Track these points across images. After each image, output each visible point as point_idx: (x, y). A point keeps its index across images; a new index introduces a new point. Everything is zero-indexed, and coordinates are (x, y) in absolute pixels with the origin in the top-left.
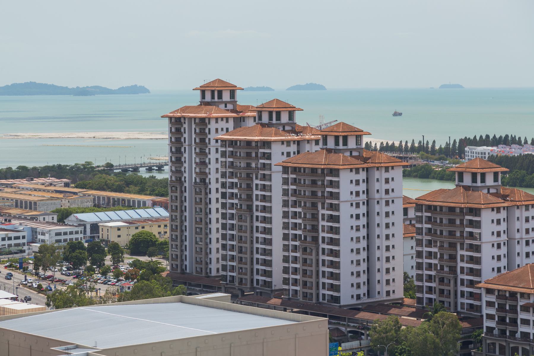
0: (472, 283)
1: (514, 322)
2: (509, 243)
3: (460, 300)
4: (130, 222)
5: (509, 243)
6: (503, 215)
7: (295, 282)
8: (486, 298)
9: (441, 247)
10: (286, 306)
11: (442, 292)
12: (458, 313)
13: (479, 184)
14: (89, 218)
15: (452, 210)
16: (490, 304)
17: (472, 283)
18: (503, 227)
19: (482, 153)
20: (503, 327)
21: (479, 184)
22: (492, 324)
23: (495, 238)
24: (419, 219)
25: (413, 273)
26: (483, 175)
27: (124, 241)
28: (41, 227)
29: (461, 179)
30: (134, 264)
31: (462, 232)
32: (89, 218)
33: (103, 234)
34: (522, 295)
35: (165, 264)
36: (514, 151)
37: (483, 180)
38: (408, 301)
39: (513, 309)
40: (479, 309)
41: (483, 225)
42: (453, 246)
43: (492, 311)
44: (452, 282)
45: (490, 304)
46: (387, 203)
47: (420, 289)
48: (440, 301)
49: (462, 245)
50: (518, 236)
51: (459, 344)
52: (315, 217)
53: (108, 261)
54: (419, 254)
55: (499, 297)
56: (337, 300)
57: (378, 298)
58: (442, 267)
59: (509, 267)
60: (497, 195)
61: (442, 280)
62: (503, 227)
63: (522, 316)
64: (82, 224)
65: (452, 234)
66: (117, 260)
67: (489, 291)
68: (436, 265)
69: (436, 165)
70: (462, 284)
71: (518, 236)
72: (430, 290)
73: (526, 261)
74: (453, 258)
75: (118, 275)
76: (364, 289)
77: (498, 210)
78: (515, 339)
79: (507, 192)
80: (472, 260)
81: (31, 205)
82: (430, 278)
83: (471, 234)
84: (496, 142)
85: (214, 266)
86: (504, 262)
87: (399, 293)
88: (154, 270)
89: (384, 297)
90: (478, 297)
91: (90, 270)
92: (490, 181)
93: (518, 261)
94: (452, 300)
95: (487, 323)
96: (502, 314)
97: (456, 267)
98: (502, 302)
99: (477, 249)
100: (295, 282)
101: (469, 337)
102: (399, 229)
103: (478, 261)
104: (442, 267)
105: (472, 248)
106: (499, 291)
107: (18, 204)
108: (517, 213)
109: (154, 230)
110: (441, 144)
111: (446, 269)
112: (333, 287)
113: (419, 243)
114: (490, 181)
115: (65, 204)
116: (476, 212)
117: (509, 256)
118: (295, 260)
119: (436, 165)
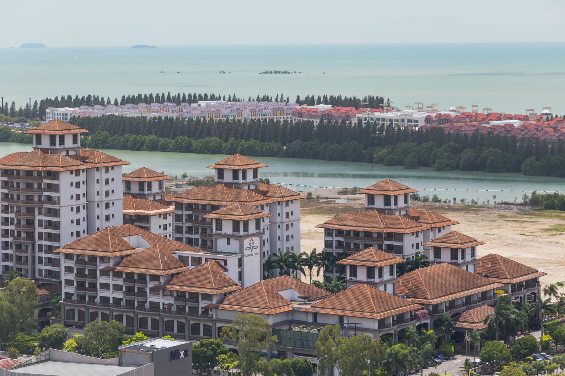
0: (50, 249)
1: (93, 286)
3: (38, 267)
5: (88, 206)
6: (82, 177)
8: (64, 263)
9: (19, 212)
11: (19, 259)
12: (36, 280)
13: (58, 146)
15: (29, 173)
16: (69, 270)
17: (50, 249)
18: (83, 189)
19: (63, 115)
20: (82, 292)
21: (58, 146)
22: (71, 290)
23: (74, 202)
26: (62, 138)
29: (39, 142)
31: (40, 197)
34: (102, 259)
36: (97, 112)
37: (62, 142)
39: (93, 274)
40: (57, 275)
41: (62, 188)
42: (30, 211)
44: (30, 249)
45: (69, 270)
46: (107, 206)
48: (18, 269)
49: (40, 209)
50: (97, 199)
51: (36, 311)
55: (77, 262)
58: (19, 233)
59: (88, 231)
60: (76, 157)
61: (19, 247)
62: (83, 189)
63: (101, 280)
65: (29, 198)
67: (68, 256)
68: (13, 231)
69: (16, 128)
70: (40, 249)
71: (97, 199)
73: (106, 224)
74: (30, 223)
77: (78, 173)
78: (94, 304)
79: (87, 154)
80: (50, 224)
83: (49, 198)
84: (78, 102)
86: (83, 226)
90: (56, 263)
92: (68, 142)
93: (98, 224)
94: (29, 267)
95: (66, 289)
96: (81, 279)
97: (33, 233)
98: (81, 266)
99: (56, 213)
101: (47, 304)
103: (56, 225)
104: (19, 233)
106: (78, 256)
108: (97, 175)
110: (20, 105)
111: (23, 235)
114: (68, 142)
116: (54, 175)
117: (88, 219)
119: (16, 128)
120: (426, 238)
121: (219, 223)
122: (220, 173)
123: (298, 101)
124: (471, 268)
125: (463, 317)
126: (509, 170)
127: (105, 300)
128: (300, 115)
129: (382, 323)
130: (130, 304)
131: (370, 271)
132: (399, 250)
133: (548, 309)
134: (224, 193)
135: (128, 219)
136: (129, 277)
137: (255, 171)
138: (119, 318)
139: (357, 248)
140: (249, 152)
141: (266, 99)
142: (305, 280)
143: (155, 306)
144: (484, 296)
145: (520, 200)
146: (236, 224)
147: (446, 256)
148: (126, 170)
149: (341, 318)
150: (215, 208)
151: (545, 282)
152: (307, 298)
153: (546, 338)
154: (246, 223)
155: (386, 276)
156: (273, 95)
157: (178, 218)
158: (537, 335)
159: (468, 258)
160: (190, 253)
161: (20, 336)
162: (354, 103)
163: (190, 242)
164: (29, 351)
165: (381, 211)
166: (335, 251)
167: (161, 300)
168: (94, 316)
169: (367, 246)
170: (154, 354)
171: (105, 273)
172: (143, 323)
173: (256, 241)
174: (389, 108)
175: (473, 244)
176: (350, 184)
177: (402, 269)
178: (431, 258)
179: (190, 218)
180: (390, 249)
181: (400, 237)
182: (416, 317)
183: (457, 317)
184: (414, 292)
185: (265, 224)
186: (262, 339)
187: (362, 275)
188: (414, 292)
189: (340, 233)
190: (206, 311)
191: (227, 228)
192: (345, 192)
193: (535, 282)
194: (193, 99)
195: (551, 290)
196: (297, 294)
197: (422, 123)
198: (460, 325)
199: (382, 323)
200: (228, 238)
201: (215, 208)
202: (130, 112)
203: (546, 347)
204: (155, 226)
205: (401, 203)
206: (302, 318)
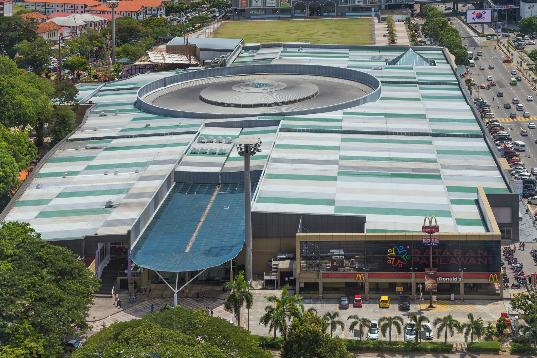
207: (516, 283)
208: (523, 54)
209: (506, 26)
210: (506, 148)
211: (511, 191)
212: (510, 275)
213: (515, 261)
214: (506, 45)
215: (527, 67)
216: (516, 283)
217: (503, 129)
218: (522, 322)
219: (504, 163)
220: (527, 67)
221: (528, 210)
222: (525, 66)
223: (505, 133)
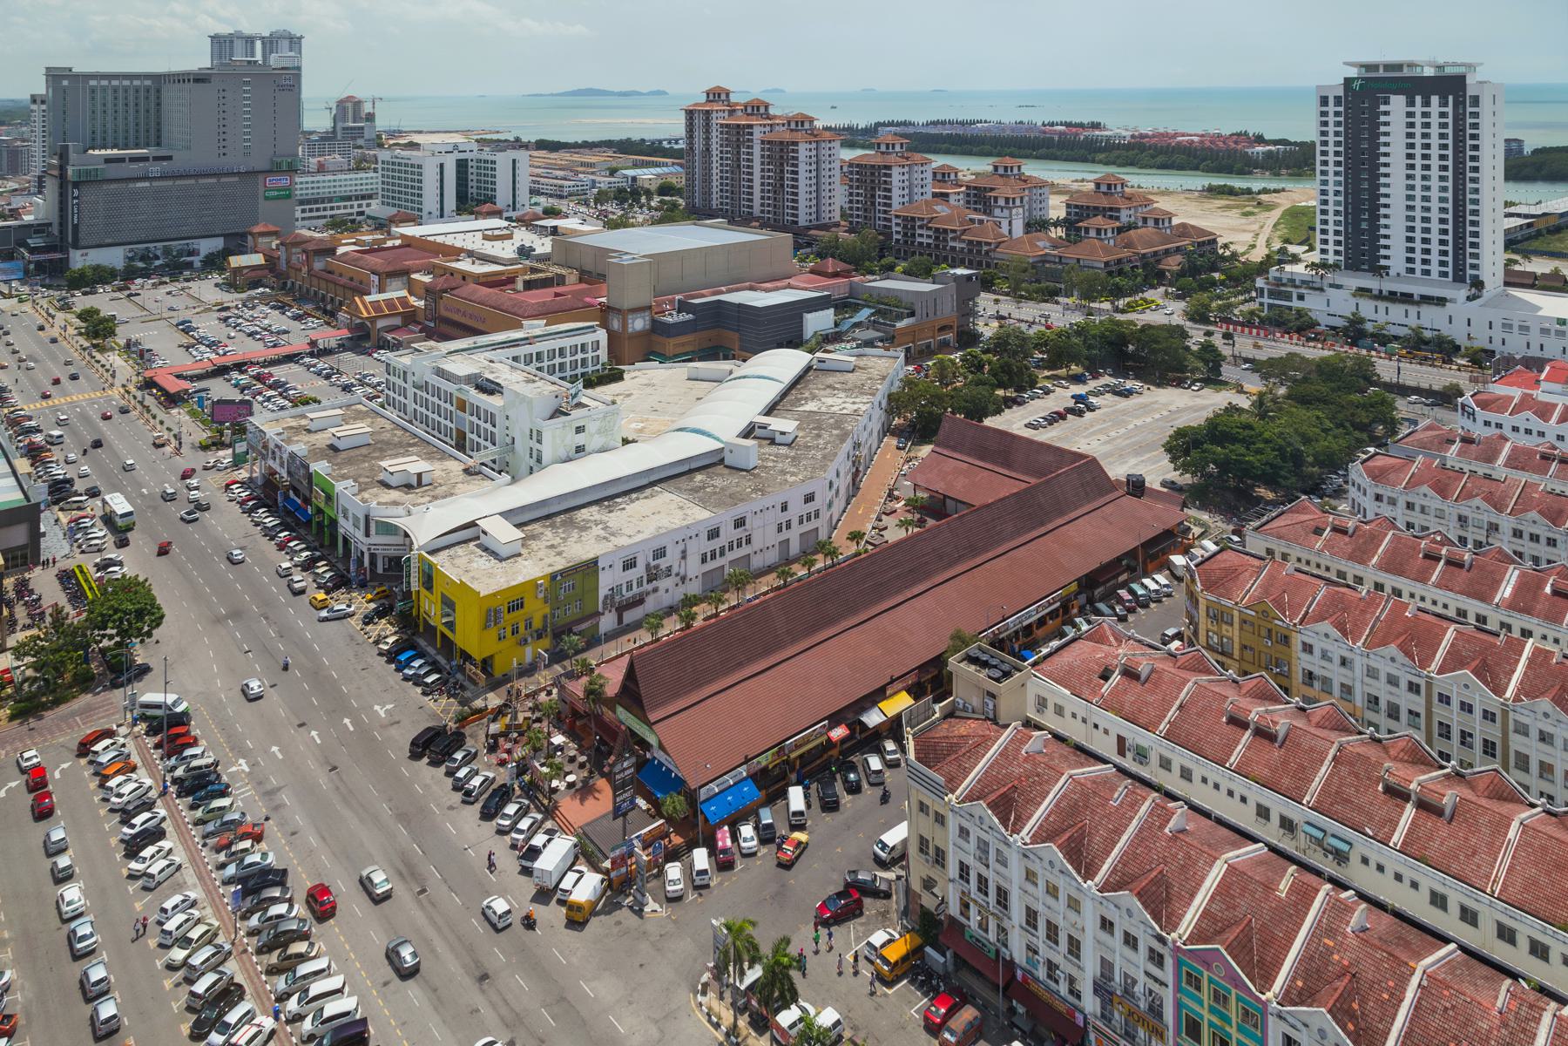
0: (885, 212)
1: (913, 235)
2: (910, 187)
4: (658, 175)
5: (910, 187)
6: (906, 169)
7: (769, 212)
8: (894, 221)
10: (761, 227)
14: (631, 173)
16: (897, 224)
17: (885, 212)
18: (906, 177)
22: (899, 237)
24: (851, 173)
25: (847, 206)
27: (653, 188)
28: (598, 179)
30: (661, 202)
32: (631, 173)
33: (639, 183)
35: (681, 201)
38: (843, 223)
39: (913, 228)
40: (890, 227)
42: (873, 189)
43: (899, 229)
45: (897, 224)
47: (851, 216)
52: (782, 171)
53: (643, 200)
54: (851, 194)
56: (796, 223)
57: (823, 221)
61: (866, 210)
62: (906, 177)
63: (919, 231)
64: (626, 177)
65: (873, 181)
66: (649, 199)
72: (858, 216)
74: (873, 196)
75: (650, 208)
76: (814, 216)
80: (886, 197)
81: (591, 165)
82: (858, 209)
83: (885, 182)
85: (714, 203)
86: (907, 198)
87: (838, 218)
88: (675, 205)
89: (827, 221)
90: (890, 220)
91: (631, 206)
95: (895, 237)
99: (889, 190)
100: (769, 212)
102: (837, 178)
103: (890, 198)
105: (886, 190)
107: (583, 164)
109: (674, 181)
112: (793, 215)
113: (851, 187)
115: (614, 164)
116: (889, 168)
117: (910, 195)
118: (769, 198)
120: (1136, 212)
121: (996, 199)
122: (996, 168)
123: (1044, 125)
124: (1168, 231)
125: (1164, 261)
126: (1191, 169)
127: (921, 244)
128: (1045, 132)
129: (1107, 264)
130: (937, 246)
131: (1098, 231)
132: (1118, 218)
133: (1223, 258)
134: (1001, 181)
135: (935, 195)
136: (937, 230)
137: (1019, 167)
138: (930, 255)
139: (1088, 217)
140: (1012, 156)
141: (1021, 122)
142: (1053, 235)
143: (953, 248)
144: (1178, 249)
145: (1200, 188)
146: (1007, 200)
147: (1151, 223)
148: (934, 165)
149: (1078, 260)
150: (992, 189)
151: (1221, 241)
152: (1055, 247)
153: (1223, 277)
154: (1014, 199)
155: (1110, 235)
156: (1025, 121)
157: (968, 195)
158: (1216, 275)
159: (1167, 224)
160: (976, 217)
161: (867, 263)
162: (1081, 125)
163: (975, 209)
164: (872, 273)
165: (1104, 193)
166: (1073, 218)
167: (958, 245)
168: (914, 253)
169: (1095, 215)
170: (956, 278)
171: (921, 227)
172: (945, 259)
173: (1021, 210)
174: (1105, 128)
175: (1170, 216)
176: (1079, 176)
177: (1120, 230)
178: (1140, 224)
179: (975, 195)
180: (1111, 217)
181: (1118, 210)
182: (1130, 261)
183: (1159, 262)
184: (1129, 245)
185: (1026, 199)
186: (1025, 271)
187: (1092, 233)
188: (1129, 245)
189: (1076, 207)
190: (987, 253)
191: (1001, 202)
192: (1076, 181)
193: (1214, 241)
194: (973, 123)
195: (1226, 246)
196: (1048, 244)
197: (1128, 139)
198: (1161, 267)
199: (1107, 264)
200: (1002, 208)
201: (992, 189)
202: (933, 131)
203: (1222, 283)
204: (952, 199)
205: (1119, 189)
206: (1052, 259)
207: (28, 621)
208: (69, 316)
209: (47, 281)
210: (32, 443)
211: (28, 500)
212: (21, 613)
213: (31, 592)
214: (45, 306)
215: (75, 332)
216: (28, 621)
217: (30, 418)
218: (30, 673)
219: (23, 465)
220: (75, 332)
221: (57, 520)
222: (71, 331)
223: (33, 423)
